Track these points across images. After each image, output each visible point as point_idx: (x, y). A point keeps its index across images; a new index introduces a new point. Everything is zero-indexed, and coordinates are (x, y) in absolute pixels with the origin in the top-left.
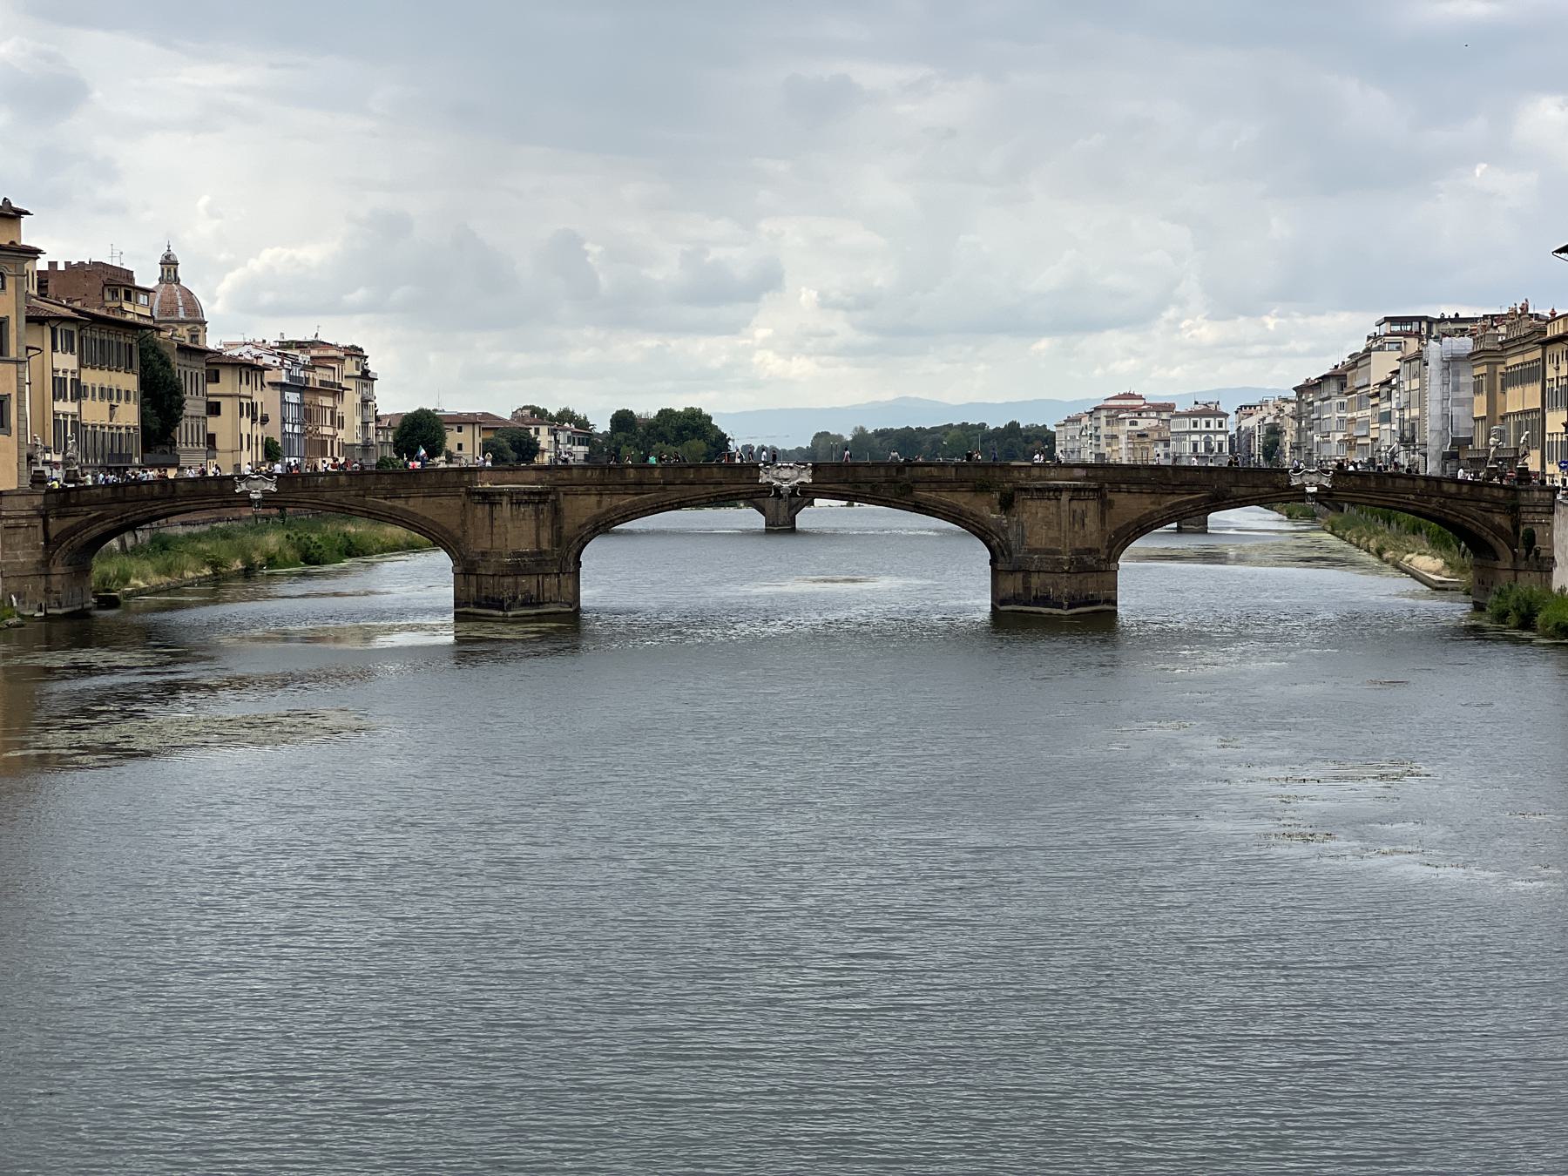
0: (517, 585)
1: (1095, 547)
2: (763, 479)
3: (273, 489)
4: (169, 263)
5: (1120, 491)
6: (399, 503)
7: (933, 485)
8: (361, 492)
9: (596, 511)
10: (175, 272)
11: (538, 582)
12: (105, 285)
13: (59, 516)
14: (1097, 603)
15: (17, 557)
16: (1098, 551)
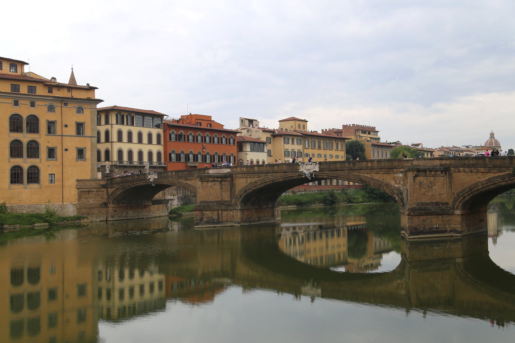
0: (203, 215)
1: (445, 201)
2: (301, 170)
3: (157, 178)
4: (492, 135)
5: (460, 172)
6: (189, 182)
7: (368, 171)
8: (178, 178)
9: (246, 184)
10: (493, 136)
11: (218, 213)
12: (356, 130)
13: (111, 188)
14: (445, 231)
15: (89, 201)
16: (447, 204)
